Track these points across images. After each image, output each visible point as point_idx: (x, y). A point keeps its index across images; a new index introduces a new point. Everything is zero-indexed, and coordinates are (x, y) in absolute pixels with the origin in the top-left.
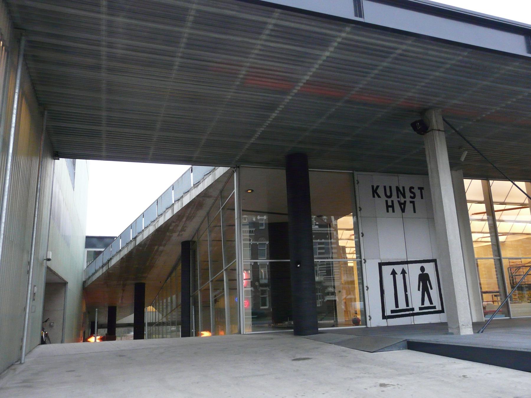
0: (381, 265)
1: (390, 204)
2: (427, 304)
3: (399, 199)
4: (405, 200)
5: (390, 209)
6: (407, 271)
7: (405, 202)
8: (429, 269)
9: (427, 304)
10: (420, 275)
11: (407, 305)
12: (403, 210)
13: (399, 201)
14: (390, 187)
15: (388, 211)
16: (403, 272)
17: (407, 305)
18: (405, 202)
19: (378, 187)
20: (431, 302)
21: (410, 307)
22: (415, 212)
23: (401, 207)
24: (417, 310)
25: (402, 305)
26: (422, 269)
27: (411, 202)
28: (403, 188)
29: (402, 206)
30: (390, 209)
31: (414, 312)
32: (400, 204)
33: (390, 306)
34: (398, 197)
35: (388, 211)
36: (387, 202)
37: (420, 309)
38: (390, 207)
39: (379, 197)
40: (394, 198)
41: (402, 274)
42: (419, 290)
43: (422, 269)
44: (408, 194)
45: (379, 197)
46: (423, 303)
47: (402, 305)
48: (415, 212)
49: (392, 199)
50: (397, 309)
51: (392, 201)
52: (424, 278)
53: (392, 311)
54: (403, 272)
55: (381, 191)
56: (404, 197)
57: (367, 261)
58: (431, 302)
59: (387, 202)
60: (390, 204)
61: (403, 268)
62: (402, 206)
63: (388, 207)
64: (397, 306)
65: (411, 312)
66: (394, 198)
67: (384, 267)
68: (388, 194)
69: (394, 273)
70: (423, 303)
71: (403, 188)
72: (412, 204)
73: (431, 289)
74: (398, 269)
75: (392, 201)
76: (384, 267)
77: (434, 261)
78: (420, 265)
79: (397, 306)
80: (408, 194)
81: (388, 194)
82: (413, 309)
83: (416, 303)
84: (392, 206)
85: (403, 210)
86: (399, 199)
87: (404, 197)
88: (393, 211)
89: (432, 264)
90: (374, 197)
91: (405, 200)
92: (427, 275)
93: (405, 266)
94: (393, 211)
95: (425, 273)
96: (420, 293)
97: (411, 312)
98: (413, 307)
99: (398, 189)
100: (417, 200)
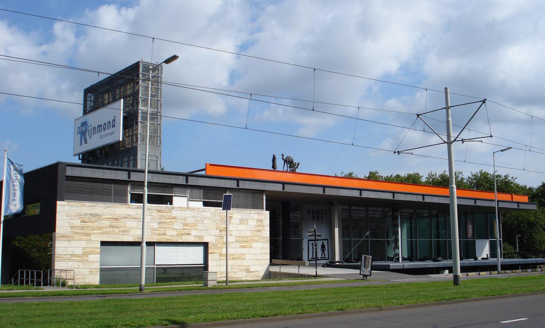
0: (309, 241)
1: (314, 216)
2: (323, 256)
5: (314, 219)
7: (319, 216)
9: (323, 256)
10: (322, 245)
12: (318, 219)
14: (314, 210)
18: (319, 216)
19: (310, 210)
21: (317, 257)
24: (319, 258)
26: (323, 243)
30: (314, 219)
36: (312, 216)
38: (313, 218)
39: (310, 214)
43: (323, 243)
44: (320, 213)
45: (310, 214)
46: (322, 256)
47: (314, 257)
51: (315, 216)
52: (323, 246)
53: (311, 258)
55: (311, 212)
56: (319, 214)
57: (304, 239)
60: (314, 216)
63: (313, 218)
67: (310, 242)
70: (322, 256)
73: (325, 250)
76: (310, 242)
78: (322, 241)
80: (320, 213)
84: (314, 218)
85: (318, 219)
88: (315, 220)
89: (326, 241)
90: (308, 214)
92: (324, 245)
94: (315, 220)
99: (317, 210)
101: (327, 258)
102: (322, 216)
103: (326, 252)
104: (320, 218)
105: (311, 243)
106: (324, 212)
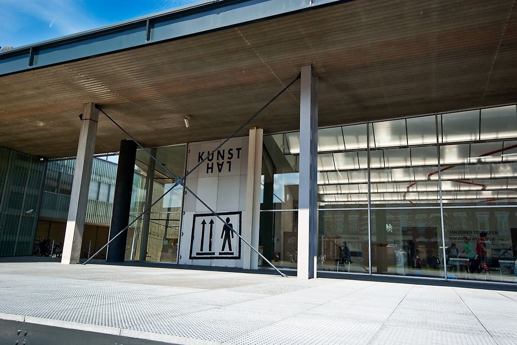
2: (227, 250)
3: (218, 161)
4: (223, 161)
5: (210, 170)
7: (223, 163)
8: (234, 220)
9: (227, 250)
11: (210, 250)
12: (220, 170)
13: (218, 163)
16: (212, 222)
17: (210, 250)
18: (223, 163)
20: (230, 250)
22: (230, 170)
23: (219, 167)
24: (217, 255)
25: (206, 249)
26: (228, 220)
27: (228, 162)
29: (220, 166)
30: (210, 170)
31: (214, 256)
32: (218, 165)
33: (197, 249)
34: (218, 159)
35: (207, 172)
36: (208, 164)
37: (220, 254)
40: (215, 161)
42: (222, 238)
44: (227, 155)
46: (223, 250)
47: (206, 249)
48: (230, 170)
49: (212, 161)
50: (202, 252)
51: (213, 164)
52: (228, 228)
53: (198, 254)
54: (212, 222)
56: (223, 158)
58: (230, 250)
59: (208, 164)
61: (212, 220)
62: (220, 166)
63: (208, 168)
64: (202, 250)
65: (212, 256)
69: (204, 223)
70: (223, 250)
71: (224, 150)
72: (228, 164)
73: (233, 237)
74: (208, 219)
75: (213, 164)
77: (240, 213)
79: (202, 250)
80: (227, 155)
83: (217, 249)
84: (212, 168)
85: (220, 170)
86: (218, 161)
87: (223, 158)
88: (212, 172)
91: (223, 161)
92: (231, 225)
94: (212, 172)
102: (229, 162)
104: (226, 166)
105: (199, 220)
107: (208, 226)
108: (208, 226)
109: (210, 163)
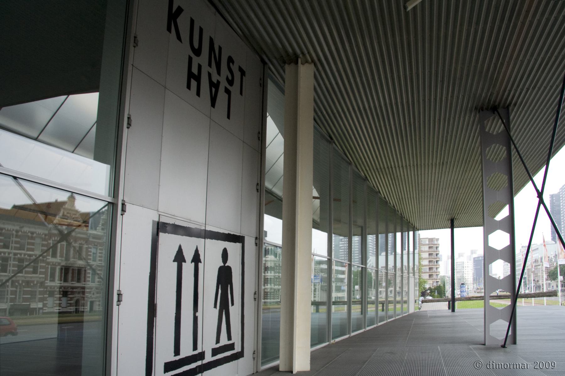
1: (195, 70)
5: (194, 83)
6: (202, 258)
7: (218, 82)
10: (221, 269)
13: (210, 75)
14: (201, 30)
15: (189, 87)
19: (180, 10)
20: (229, 338)
24: (209, 358)
25: (186, 351)
28: (220, 48)
29: (214, 90)
30: (194, 83)
31: (205, 361)
34: (210, 65)
35: (189, 87)
36: (190, 59)
37: (215, 352)
41: (193, 263)
43: (225, 255)
46: (218, 341)
50: (177, 358)
51: (200, 67)
54: (196, 259)
57: (128, 207)
58: (229, 338)
59: (190, 59)
60: (195, 70)
62: (214, 90)
63: (190, 75)
64: (177, 351)
65: (199, 363)
66: (203, 59)
68: (196, 46)
69: (179, 258)
70: (218, 341)
71: (220, 48)
73: (233, 304)
75: (200, 67)
79: (177, 351)
81: (196, 46)
82: (201, 356)
84: (198, 79)
86: (210, 70)
88: (198, 94)
90: (169, 30)
92: (229, 268)
93: (200, 242)
95: (227, 266)
96: (217, 311)
97: (199, 363)
98: (203, 350)
100: (234, 90)
101: (238, 349)
102: (228, 91)
103: (234, 311)
104: (222, 97)
106: (237, 75)
107: (188, 268)
108: (188, 268)
109: (196, 61)
